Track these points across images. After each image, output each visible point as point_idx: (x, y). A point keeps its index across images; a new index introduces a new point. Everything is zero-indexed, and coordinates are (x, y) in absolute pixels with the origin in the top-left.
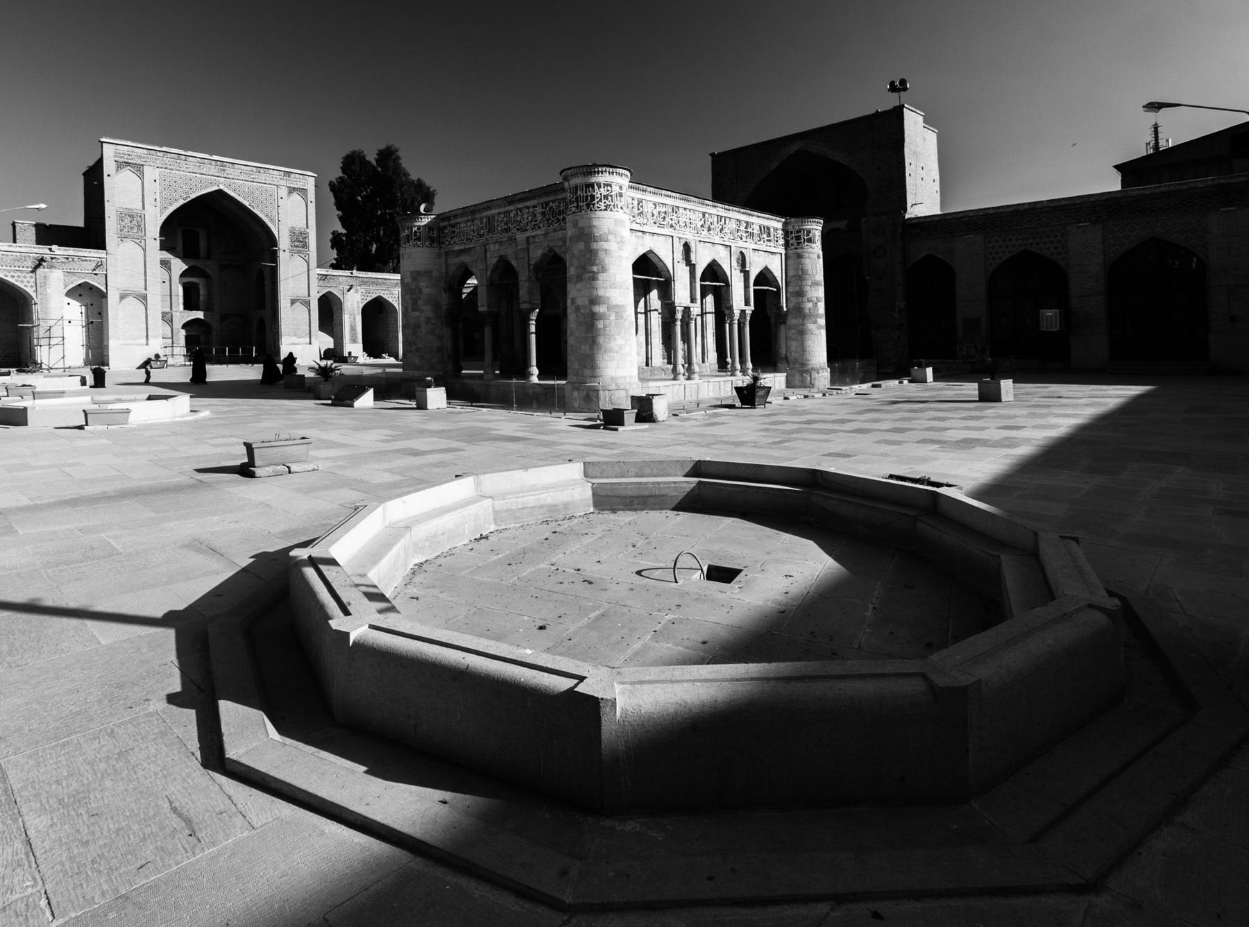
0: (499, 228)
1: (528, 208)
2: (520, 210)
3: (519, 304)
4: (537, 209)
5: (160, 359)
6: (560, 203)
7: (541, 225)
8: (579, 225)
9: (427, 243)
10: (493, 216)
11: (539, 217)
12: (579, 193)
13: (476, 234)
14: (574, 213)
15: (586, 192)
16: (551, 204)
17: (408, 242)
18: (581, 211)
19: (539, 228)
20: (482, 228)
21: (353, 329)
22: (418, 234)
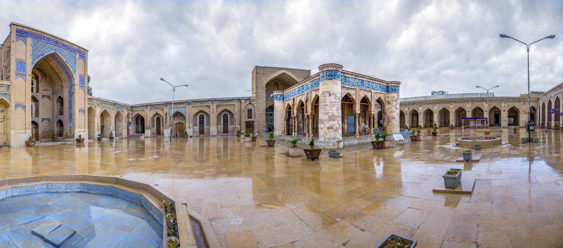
1: (375, 83)
2: (373, 82)
5: (240, 131)
13: (356, 84)
20: (359, 83)
21: (98, 124)
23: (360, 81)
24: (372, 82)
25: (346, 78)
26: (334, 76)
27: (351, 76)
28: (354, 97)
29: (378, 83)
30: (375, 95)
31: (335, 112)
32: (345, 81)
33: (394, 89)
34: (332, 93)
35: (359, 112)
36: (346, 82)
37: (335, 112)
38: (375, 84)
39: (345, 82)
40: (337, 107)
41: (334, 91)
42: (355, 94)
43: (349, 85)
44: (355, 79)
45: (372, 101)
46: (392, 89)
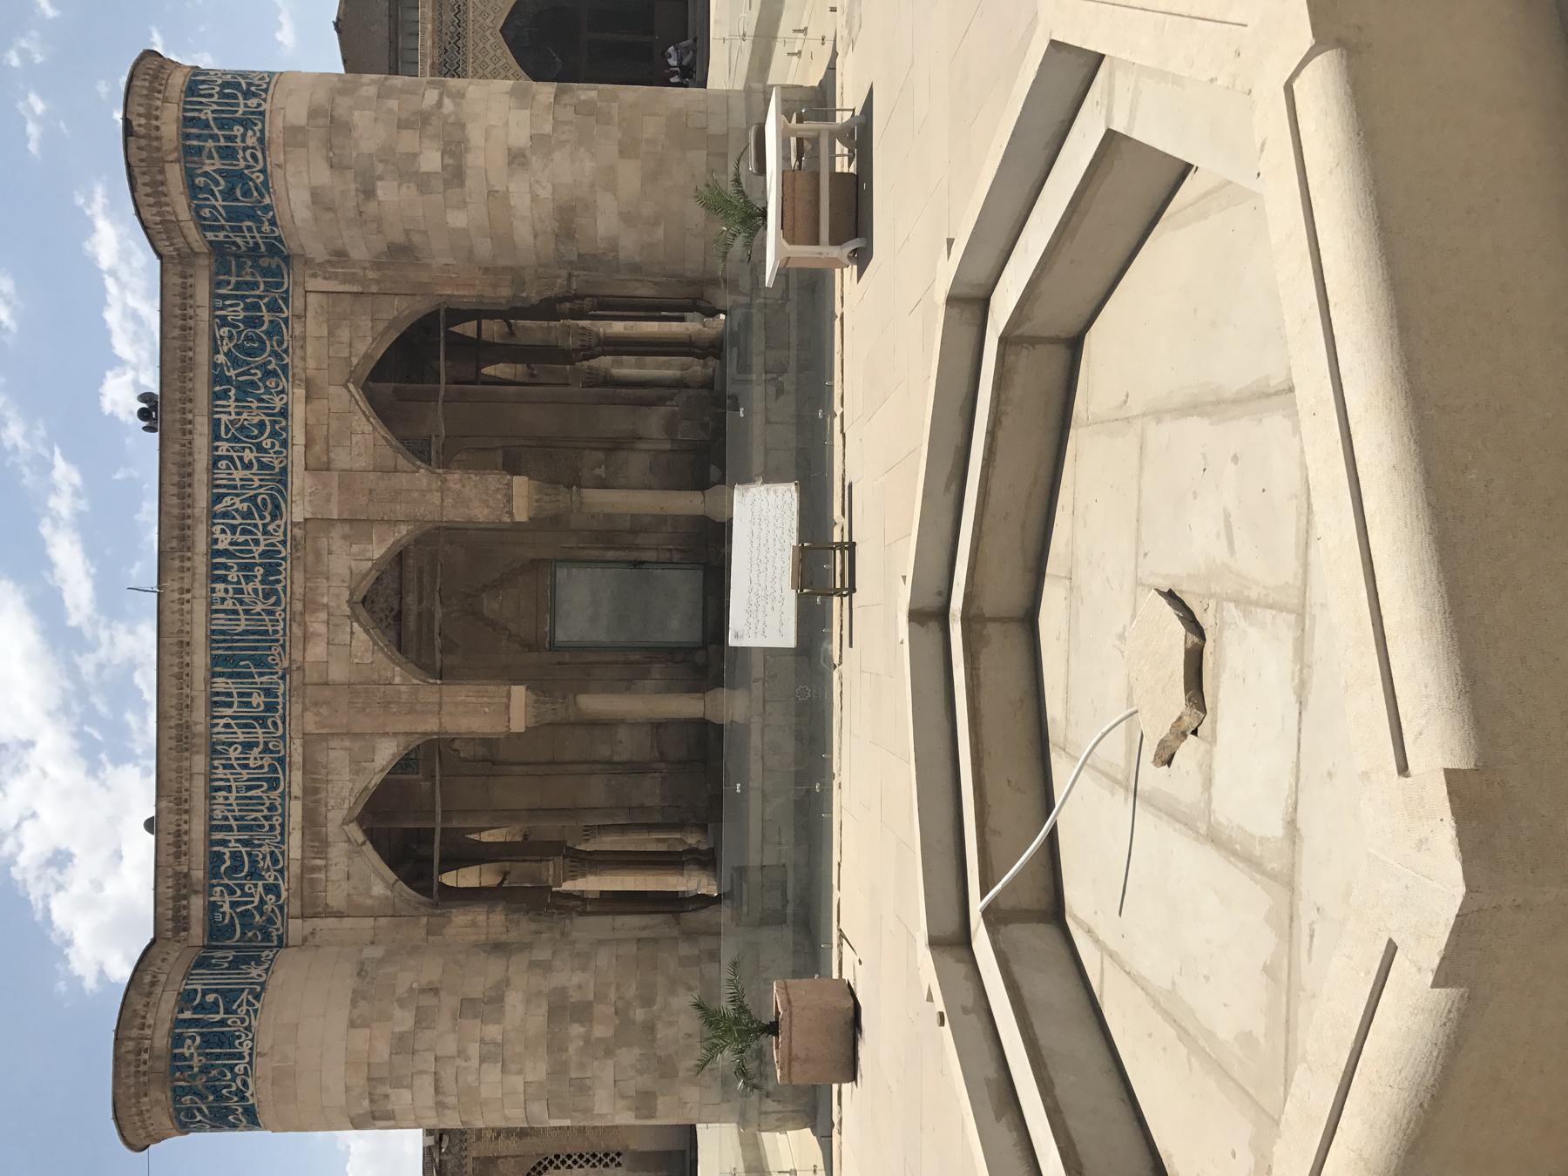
0: (258, 608)
1: (215, 461)
3: (512, 737)
4: (224, 418)
6: (224, 322)
7: (278, 404)
8: (302, 121)
9: (254, 972)
10: (214, 636)
11: (251, 418)
12: (207, 115)
14: (261, 140)
15: (211, 96)
16: (221, 358)
17: (226, 1040)
18: (262, 113)
19: (284, 413)
22: (210, 998)
23: (221, 684)
24: (213, 516)
25: (220, 855)
26: (219, 1097)
27: (199, 802)
28: (386, 753)
29: (202, 426)
30: (341, 458)
31: (517, 1082)
32: (251, 875)
33: (229, 194)
34: (366, 1103)
35: (520, 484)
36: (254, 862)
37: (517, 1082)
38: (221, 475)
39: (254, 874)
40: (475, 1062)
41: (347, 1089)
42: (357, 745)
43: (276, 821)
44: (213, 752)
45: (401, 510)
46: (234, 215)
